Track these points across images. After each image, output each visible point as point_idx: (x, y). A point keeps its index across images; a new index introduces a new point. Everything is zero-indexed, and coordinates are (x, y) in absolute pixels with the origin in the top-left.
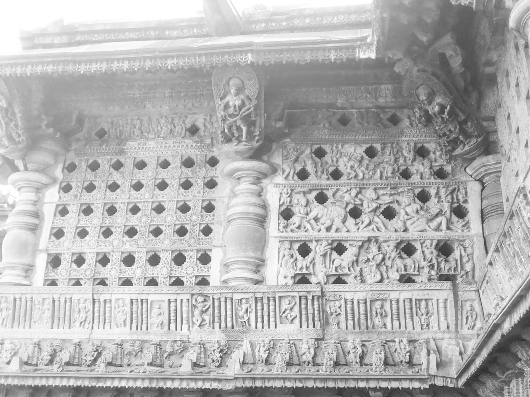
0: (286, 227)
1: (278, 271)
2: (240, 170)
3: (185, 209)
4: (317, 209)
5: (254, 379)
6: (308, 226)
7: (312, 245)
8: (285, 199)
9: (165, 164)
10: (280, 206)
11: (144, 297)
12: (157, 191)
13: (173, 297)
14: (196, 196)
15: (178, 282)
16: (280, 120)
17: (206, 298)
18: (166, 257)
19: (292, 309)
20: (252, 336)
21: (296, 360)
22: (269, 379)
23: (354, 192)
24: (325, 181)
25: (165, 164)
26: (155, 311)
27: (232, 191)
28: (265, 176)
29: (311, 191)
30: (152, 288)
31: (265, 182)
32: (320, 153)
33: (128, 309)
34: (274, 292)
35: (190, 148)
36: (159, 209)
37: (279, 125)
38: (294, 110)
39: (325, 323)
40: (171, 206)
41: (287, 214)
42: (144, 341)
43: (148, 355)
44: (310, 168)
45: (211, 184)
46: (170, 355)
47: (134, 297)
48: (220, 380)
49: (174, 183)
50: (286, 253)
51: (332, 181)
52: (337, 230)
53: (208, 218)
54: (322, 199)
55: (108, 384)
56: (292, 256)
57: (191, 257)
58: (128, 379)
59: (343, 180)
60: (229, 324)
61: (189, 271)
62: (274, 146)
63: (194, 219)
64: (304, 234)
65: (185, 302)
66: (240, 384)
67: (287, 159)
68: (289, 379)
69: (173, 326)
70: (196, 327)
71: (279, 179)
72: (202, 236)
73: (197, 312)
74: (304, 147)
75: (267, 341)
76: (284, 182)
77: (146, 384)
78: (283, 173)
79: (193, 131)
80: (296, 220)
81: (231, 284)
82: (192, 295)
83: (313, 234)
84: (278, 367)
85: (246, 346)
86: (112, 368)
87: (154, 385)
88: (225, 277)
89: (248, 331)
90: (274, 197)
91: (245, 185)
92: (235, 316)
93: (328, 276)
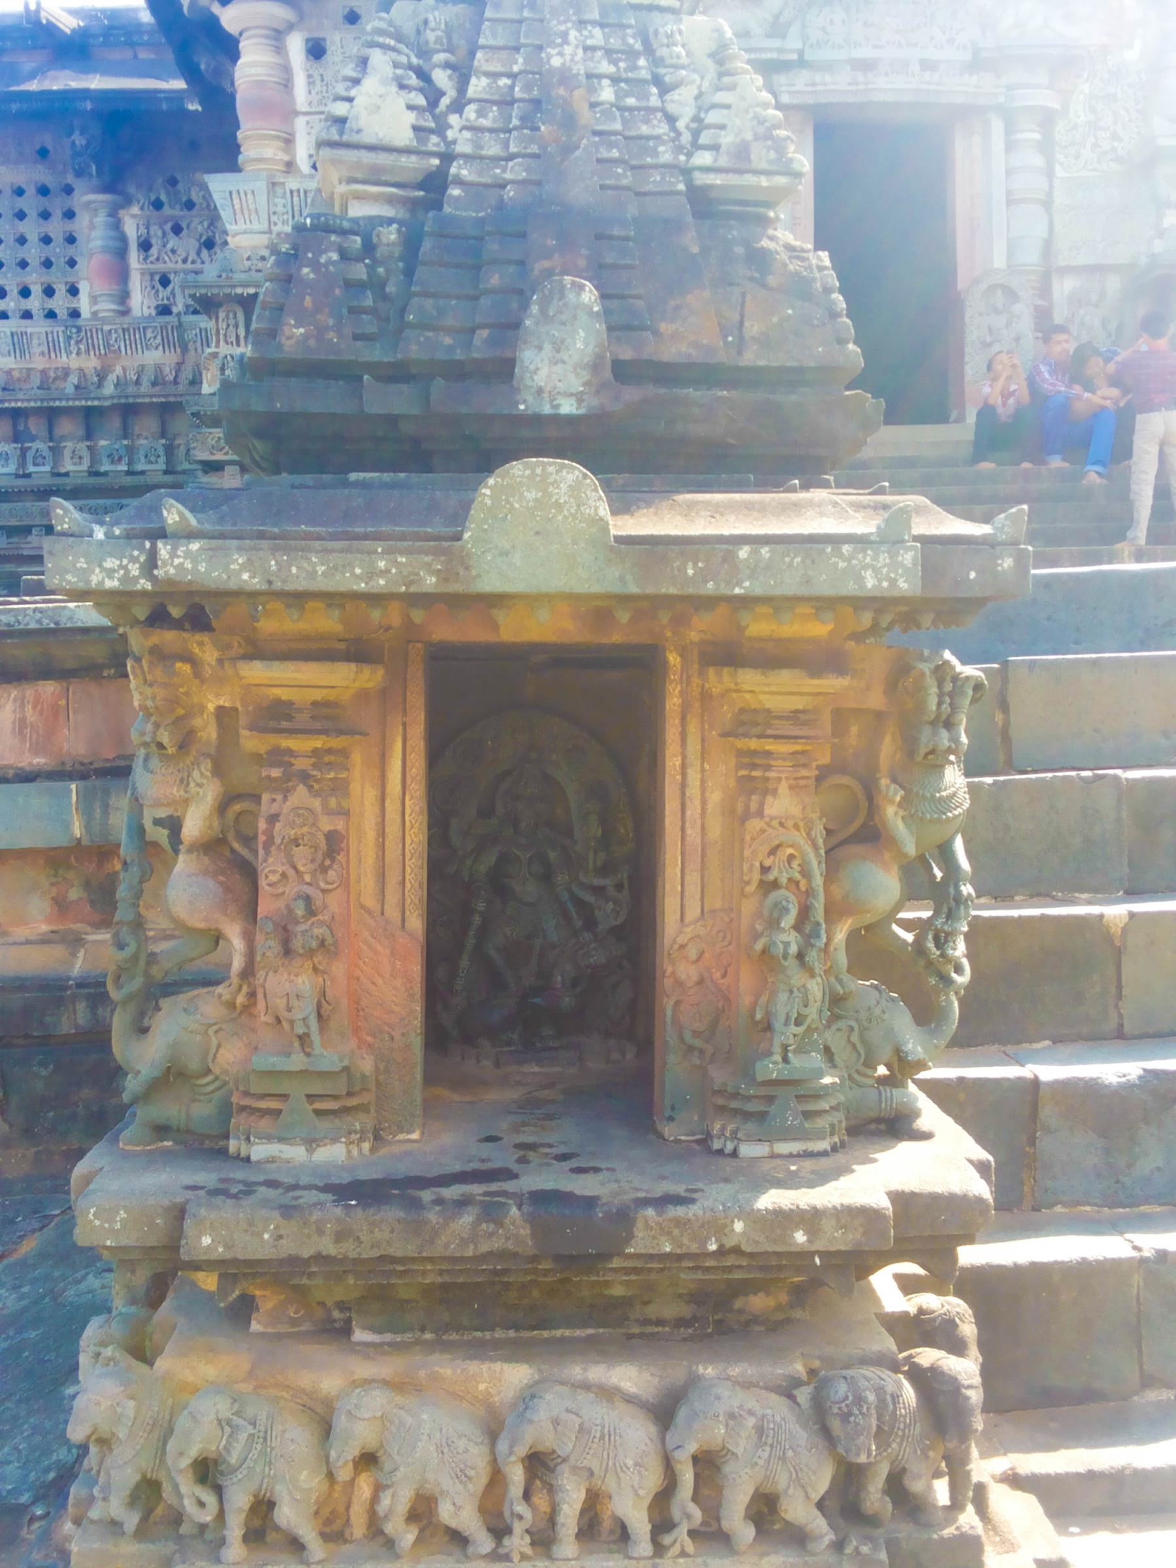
0: (145, 259)
1: (141, 302)
2: (94, 202)
3: (46, 240)
4: (173, 242)
5: (127, 397)
6: (166, 258)
7: (172, 277)
8: (143, 230)
9: (20, 192)
10: (139, 237)
11: (23, 330)
12: (17, 221)
13: (49, 329)
14: (56, 228)
15: (51, 315)
17: (79, 329)
18: (37, 290)
19: (155, 338)
21: (160, 380)
22: (139, 396)
23: (206, 224)
24: (177, 212)
25: (20, 192)
26: (35, 341)
27: (91, 222)
28: (122, 207)
29: (166, 222)
30: (28, 322)
31: (122, 213)
32: (173, 182)
33: (9, 340)
35: (41, 174)
36: (22, 240)
39: (185, 350)
40: (33, 237)
41: (145, 246)
42: (29, 369)
43: (36, 381)
44: (163, 197)
45: (70, 215)
46: (55, 379)
47: (14, 330)
48: (98, 399)
49: (32, 214)
50: (148, 284)
51: (185, 212)
52: (193, 262)
53: (71, 251)
54: (177, 230)
55: (6, 405)
56: (153, 287)
57: (61, 290)
58: (23, 401)
59: (194, 212)
60: (103, 352)
61: (60, 302)
63: (57, 251)
64: (163, 266)
65: (60, 334)
66: (115, 401)
68: (155, 396)
69: (53, 355)
70: (74, 355)
71: (135, 210)
72: (67, 268)
73: (72, 342)
75: (136, 365)
77: (39, 404)
79: (43, 153)
80: (154, 251)
81: (101, 315)
82: (66, 327)
83: (170, 266)
84: (145, 388)
86: (7, 393)
87: (45, 404)
88: (95, 308)
90: (131, 229)
91: (101, 218)
92: (108, 346)
93: (187, 307)
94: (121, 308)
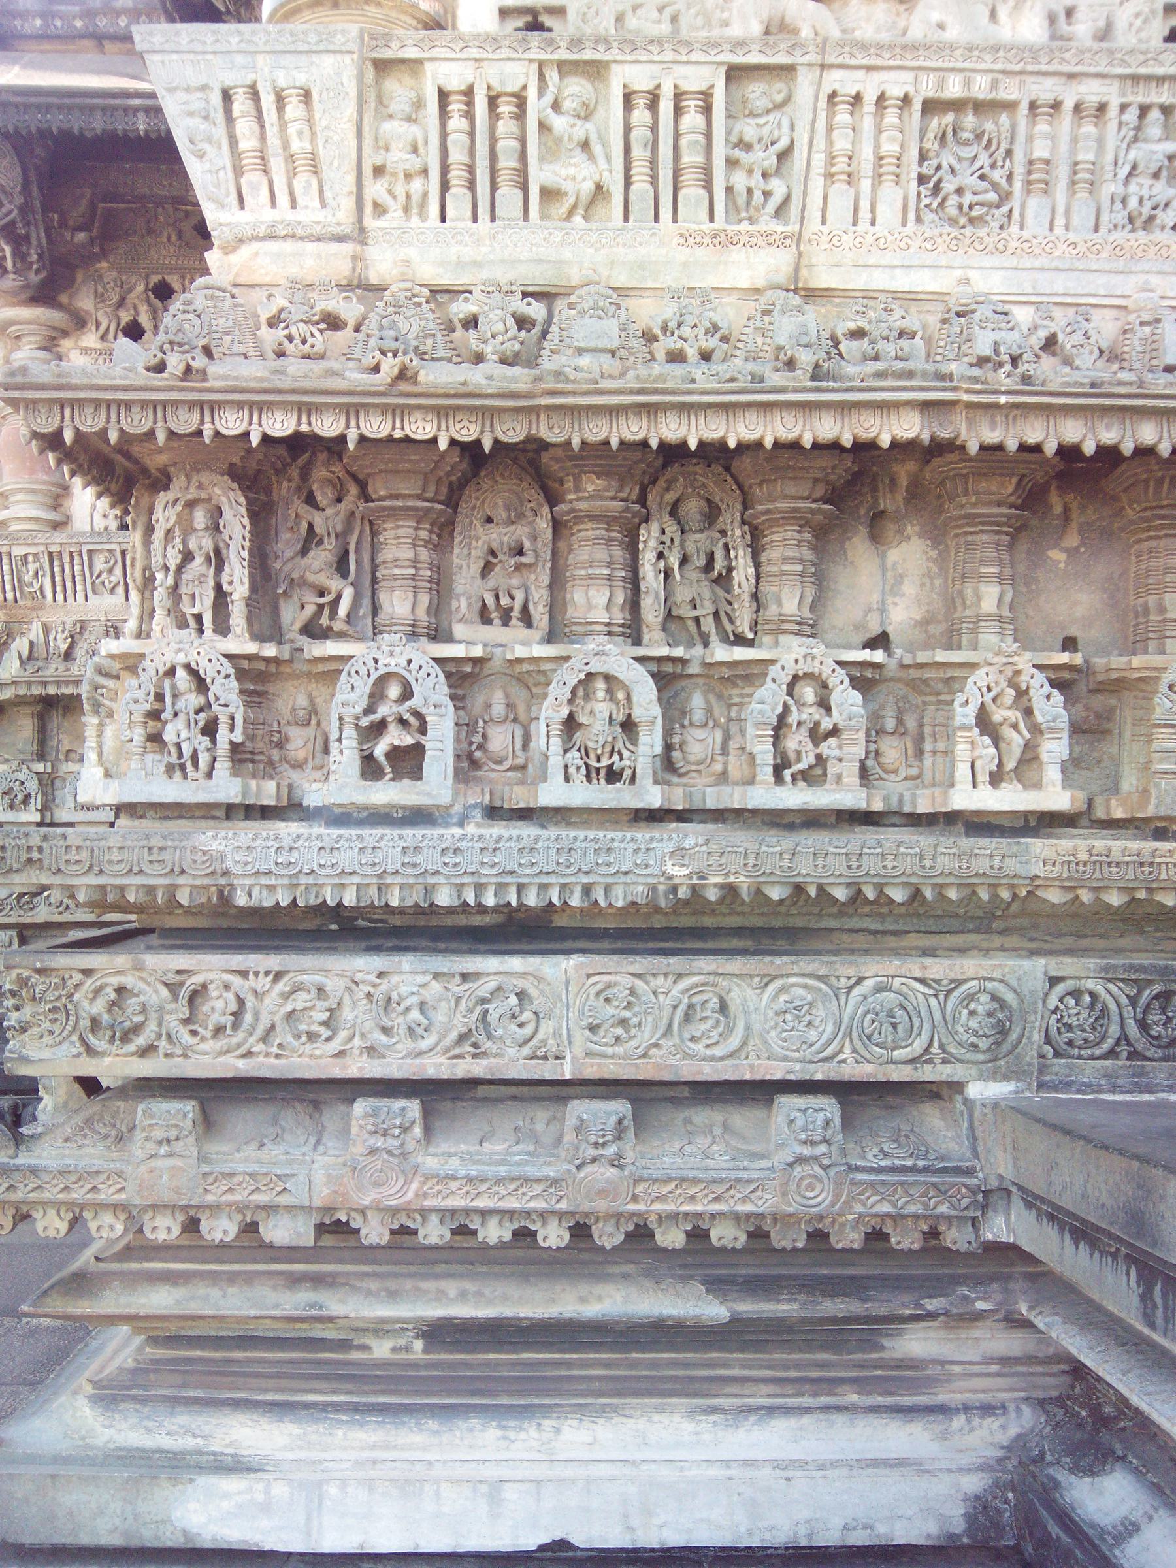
16: (80, 229)
20: (48, 616)
28: (65, 333)
31: (66, 344)
34: (80, 544)
37: (81, 236)
38: (114, 205)
62: (80, 276)
66: (22, 691)
67: (104, 301)
71: (90, 339)
74: (134, 279)
76: (98, 345)
78: (97, 328)
85: (35, 632)
89: (42, 607)
94: (52, 516)
